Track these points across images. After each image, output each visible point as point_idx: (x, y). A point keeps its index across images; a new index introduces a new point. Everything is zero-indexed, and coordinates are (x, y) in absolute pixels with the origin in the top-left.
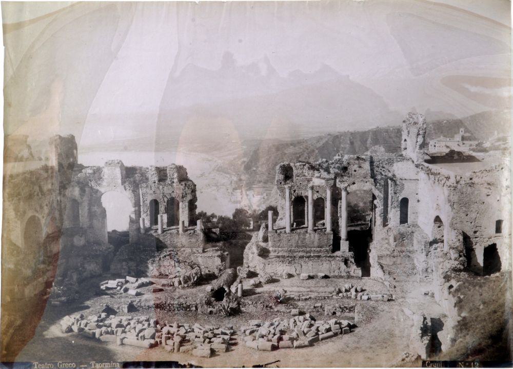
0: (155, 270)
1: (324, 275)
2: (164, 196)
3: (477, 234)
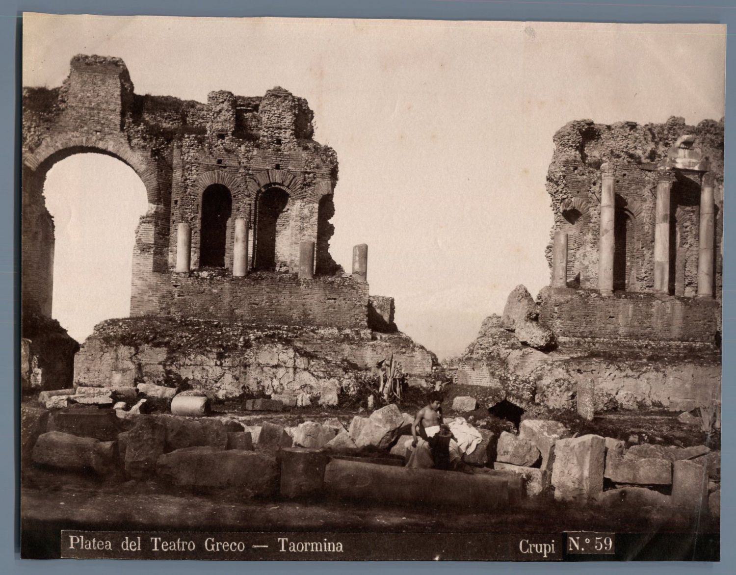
0: (228, 377)
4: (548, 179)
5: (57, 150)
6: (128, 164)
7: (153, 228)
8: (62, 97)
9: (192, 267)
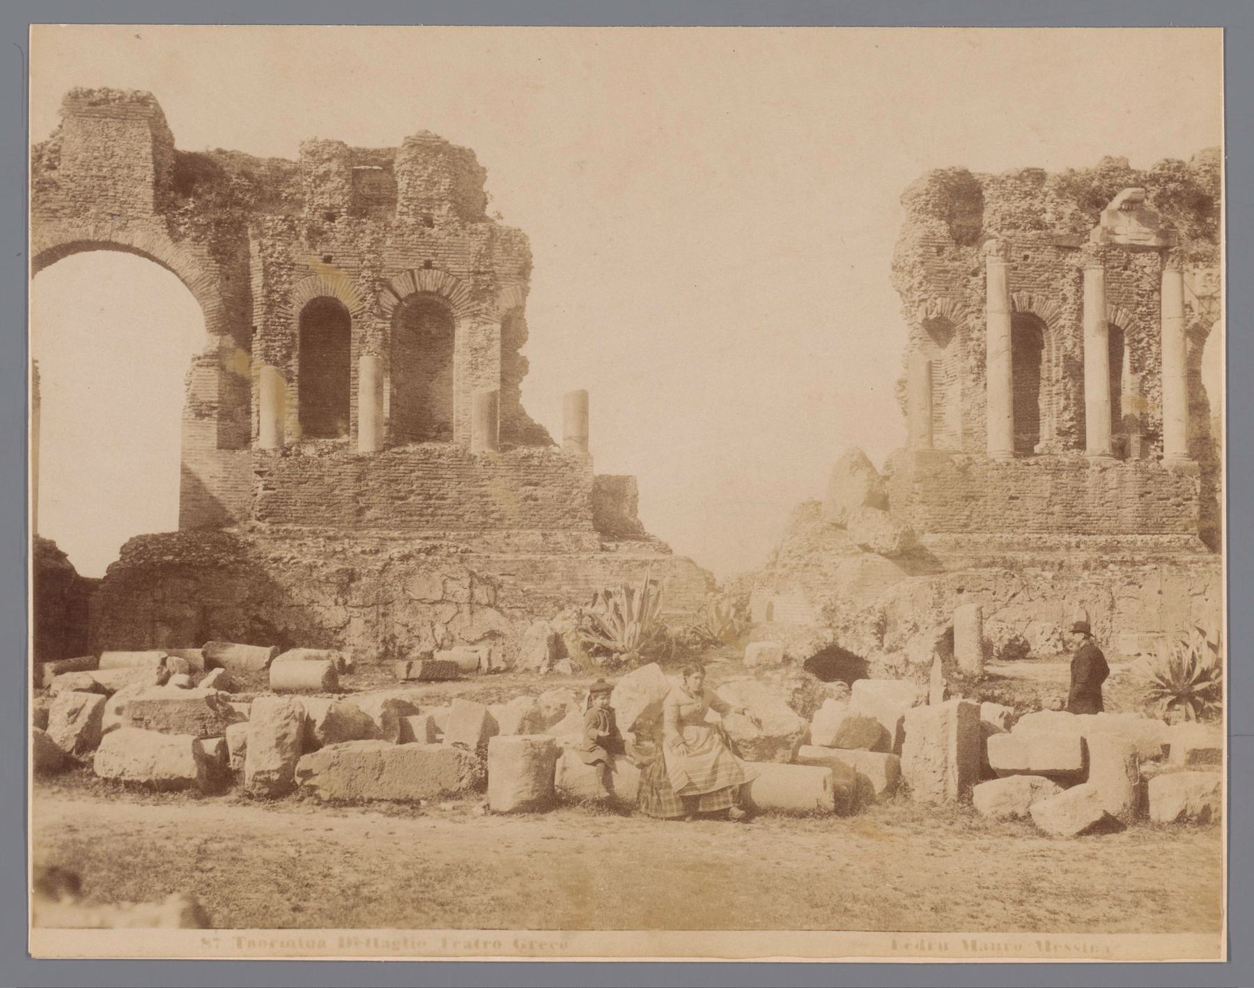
2: (381, 284)
4: (894, 268)
5: (43, 249)
6: (169, 268)
7: (216, 377)
8: (49, 160)
9: (287, 440)
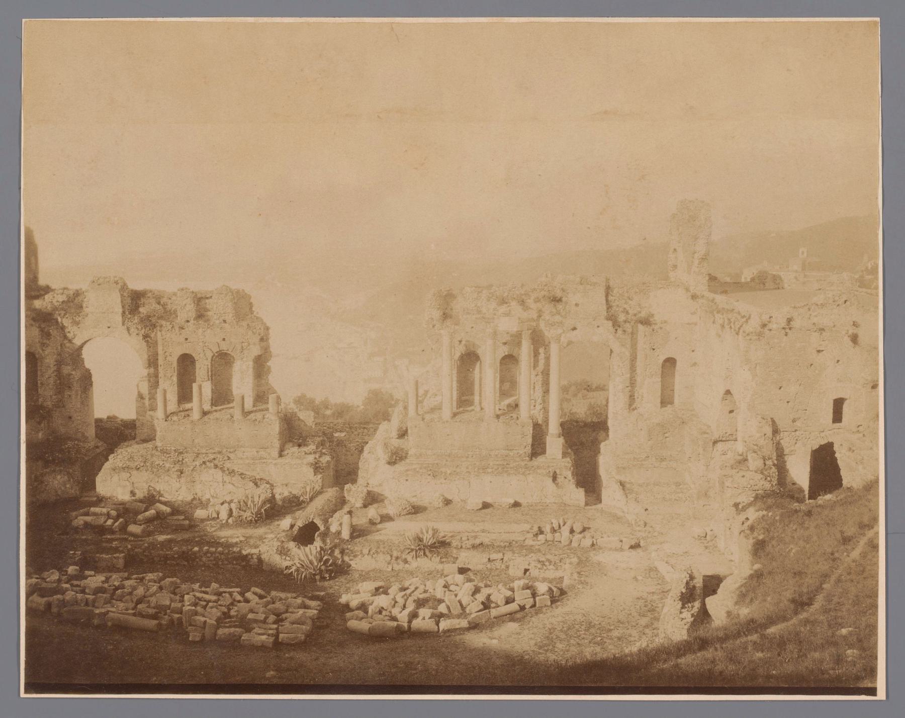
0: (184, 488)
1: (512, 501)
3: (798, 423)
